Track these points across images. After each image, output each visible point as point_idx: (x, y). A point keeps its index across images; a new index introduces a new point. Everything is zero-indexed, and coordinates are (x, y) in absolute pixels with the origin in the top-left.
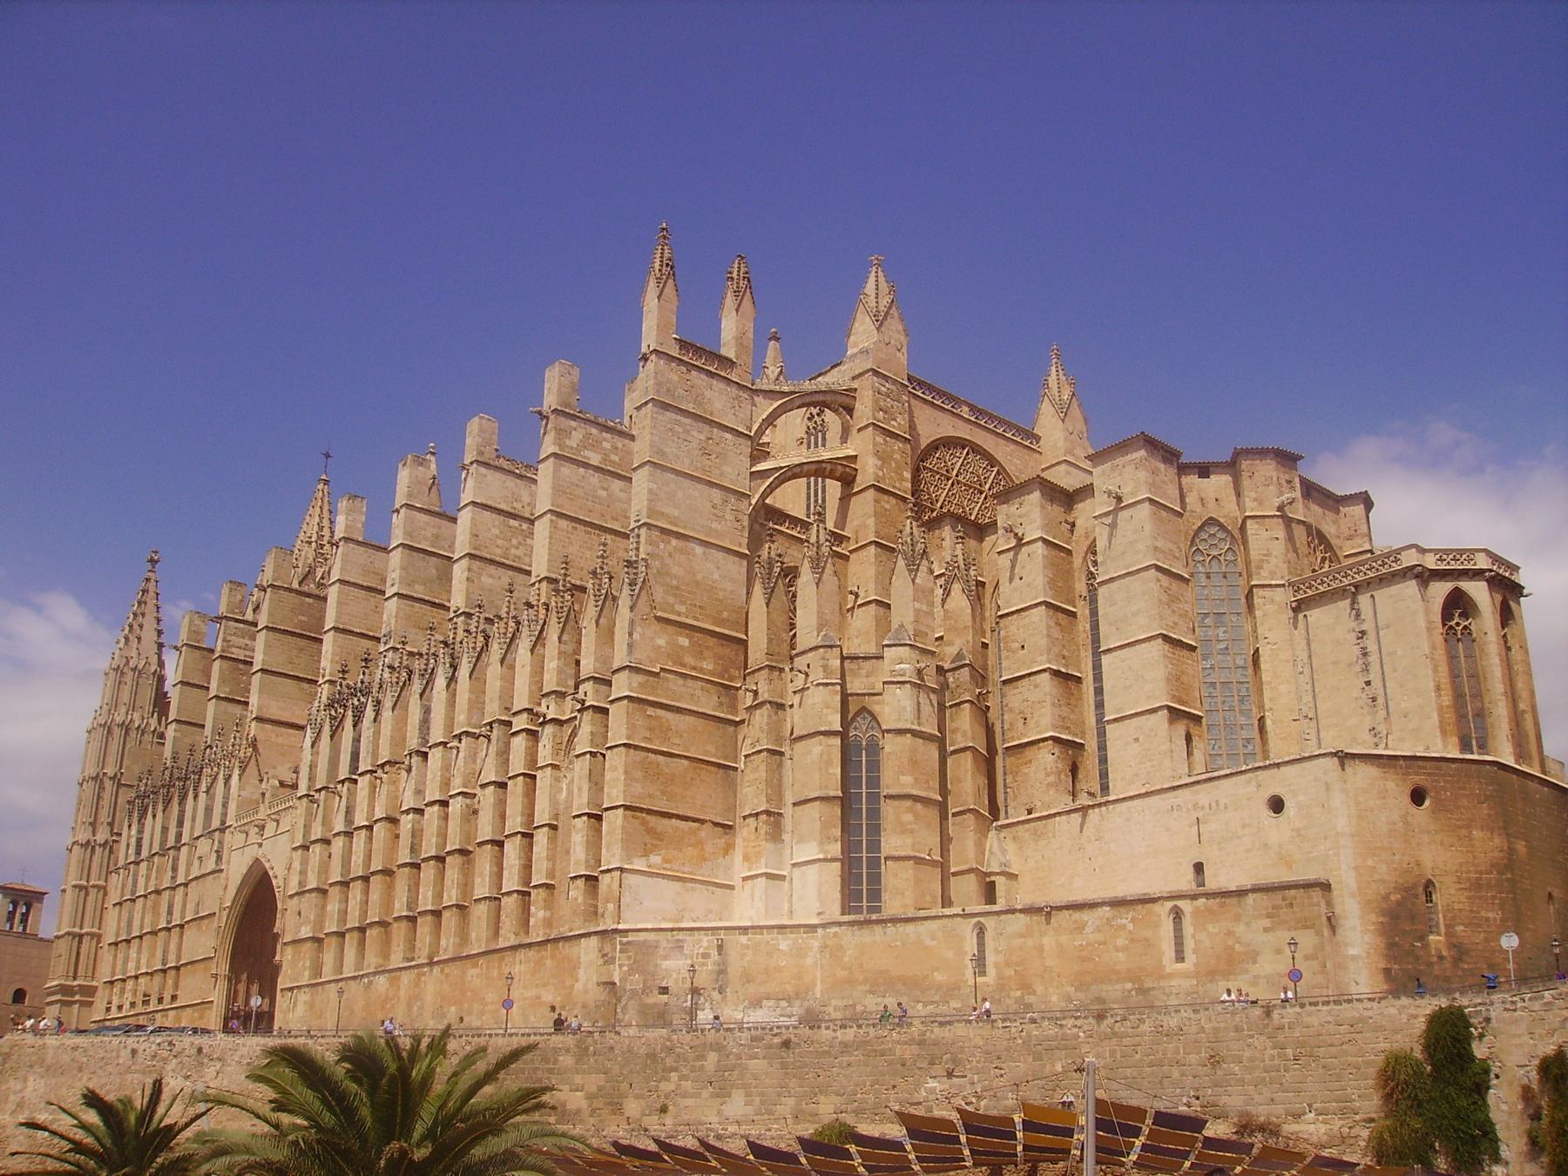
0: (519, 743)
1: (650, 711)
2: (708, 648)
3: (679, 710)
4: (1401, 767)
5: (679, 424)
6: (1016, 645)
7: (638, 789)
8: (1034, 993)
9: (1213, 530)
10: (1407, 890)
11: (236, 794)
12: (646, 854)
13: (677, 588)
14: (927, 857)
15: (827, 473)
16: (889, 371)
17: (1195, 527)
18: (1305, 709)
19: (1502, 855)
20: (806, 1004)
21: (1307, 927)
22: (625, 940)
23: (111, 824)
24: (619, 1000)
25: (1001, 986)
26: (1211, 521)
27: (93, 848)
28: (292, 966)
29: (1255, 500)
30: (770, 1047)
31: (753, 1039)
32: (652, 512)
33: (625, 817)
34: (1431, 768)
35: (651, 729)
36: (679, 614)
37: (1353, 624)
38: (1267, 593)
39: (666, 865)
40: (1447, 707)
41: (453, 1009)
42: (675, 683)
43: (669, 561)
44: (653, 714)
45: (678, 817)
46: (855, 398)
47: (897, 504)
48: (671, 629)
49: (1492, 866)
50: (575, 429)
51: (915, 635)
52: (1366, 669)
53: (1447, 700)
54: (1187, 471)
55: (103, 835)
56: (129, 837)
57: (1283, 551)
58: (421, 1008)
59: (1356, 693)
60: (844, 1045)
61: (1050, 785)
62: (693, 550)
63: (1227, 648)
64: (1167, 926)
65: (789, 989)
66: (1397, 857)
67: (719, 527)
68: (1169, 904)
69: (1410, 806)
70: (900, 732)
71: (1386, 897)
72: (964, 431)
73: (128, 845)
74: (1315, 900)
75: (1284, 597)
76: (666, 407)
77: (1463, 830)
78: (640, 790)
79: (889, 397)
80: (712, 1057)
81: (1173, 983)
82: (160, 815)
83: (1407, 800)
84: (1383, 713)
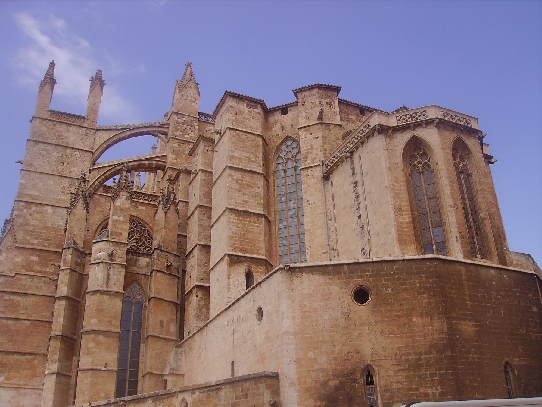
1: (6, 297)
3: (26, 294)
4: (345, 273)
5: (45, 150)
6: (191, 234)
9: (289, 143)
10: (345, 376)
13: (33, 231)
14: (103, 369)
15: (147, 166)
17: (278, 144)
18: (332, 244)
19: (441, 336)
26: (288, 138)
34: (373, 271)
35: (5, 307)
36: (33, 244)
37: (352, 179)
38: (309, 172)
40: (407, 223)
42: (25, 281)
43: (29, 218)
44: (7, 298)
46: (168, 128)
48: (26, 253)
49: (431, 346)
51: (111, 235)
52: (358, 208)
53: (406, 218)
54: (275, 113)
59: (355, 226)
62: (47, 211)
63: (295, 214)
66: (338, 348)
67: (66, 198)
68: (180, 397)
69: (352, 304)
70: (94, 292)
71: (325, 384)
74: (261, 391)
75: (318, 173)
76: (37, 142)
77: (402, 319)
79: (184, 124)
83: (349, 299)
84: (366, 238)
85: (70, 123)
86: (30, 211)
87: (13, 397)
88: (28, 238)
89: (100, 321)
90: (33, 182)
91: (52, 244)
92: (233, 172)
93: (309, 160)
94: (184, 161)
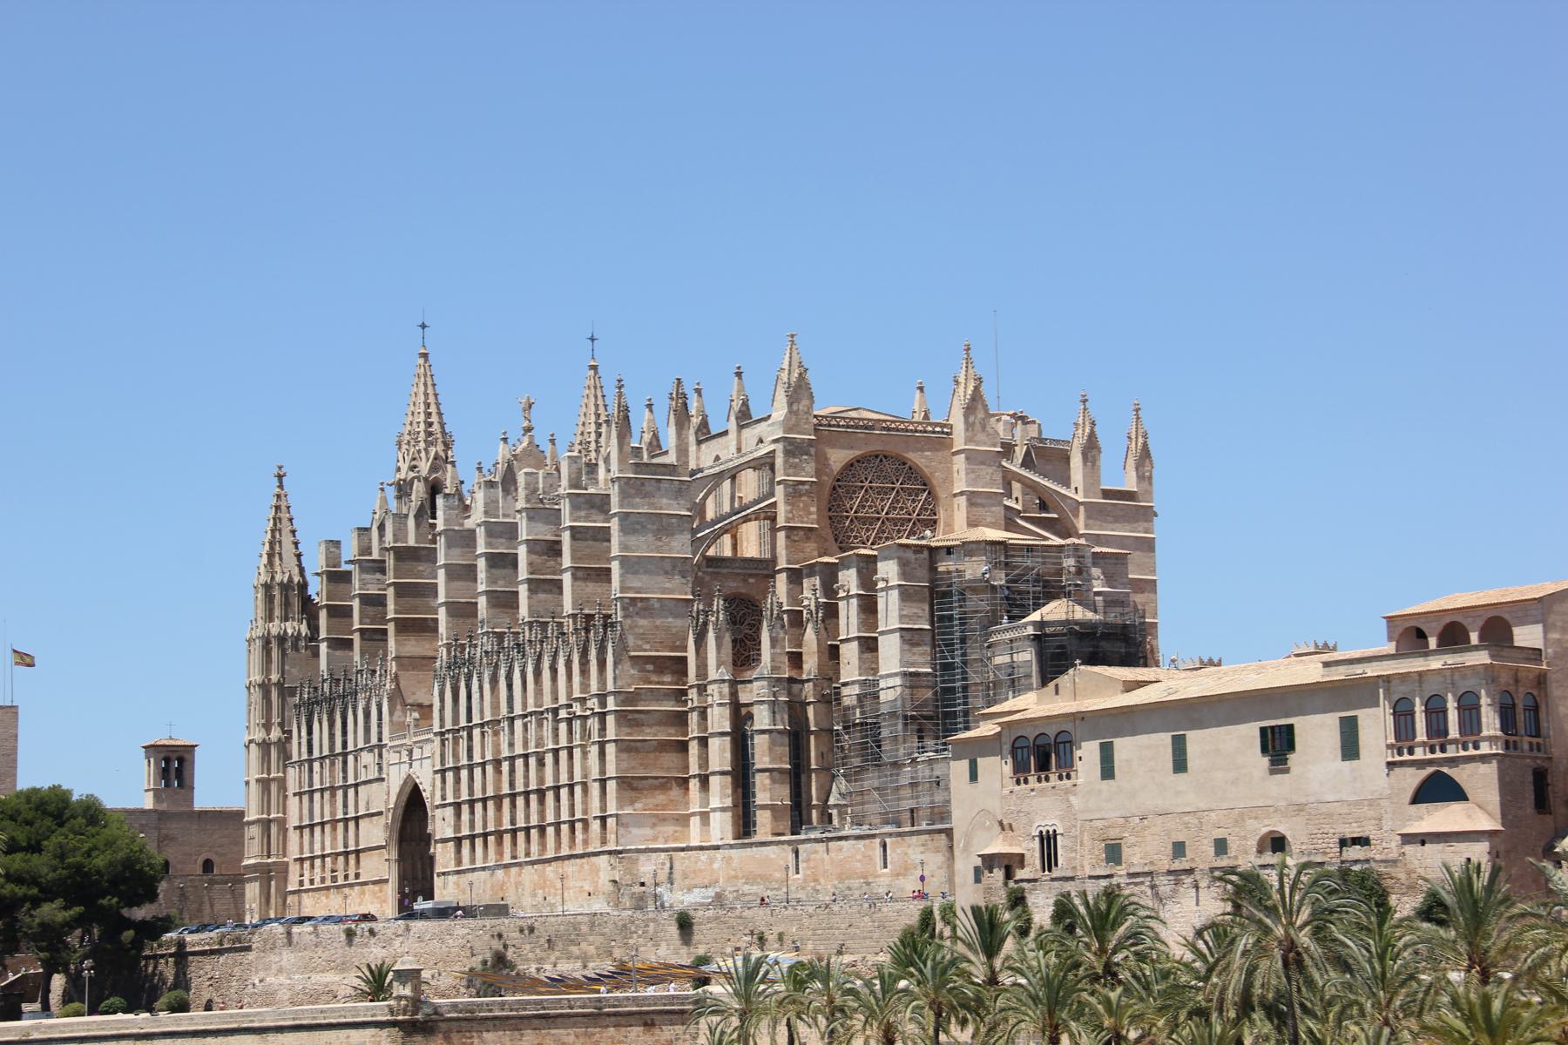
0: (563, 727)
2: (666, 668)
5: (638, 523)
6: (846, 661)
7: (624, 765)
12: (632, 803)
13: (643, 634)
21: (938, 852)
23: (281, 725)
24: (619, 890)
25: (805, 881)
28: (443, 856)
41: (540, 891)
45: (652, 777)
55: (275, 734)
58: (523, 890)
60: (708, 918)
64: (878, 851)
65: (706, 882)
70: (763, 732)
73: (300, 743)
80: (652, 925)
81: (882, 879)
86: (637, 610)
88: (640, 643)
91: (665, 647)
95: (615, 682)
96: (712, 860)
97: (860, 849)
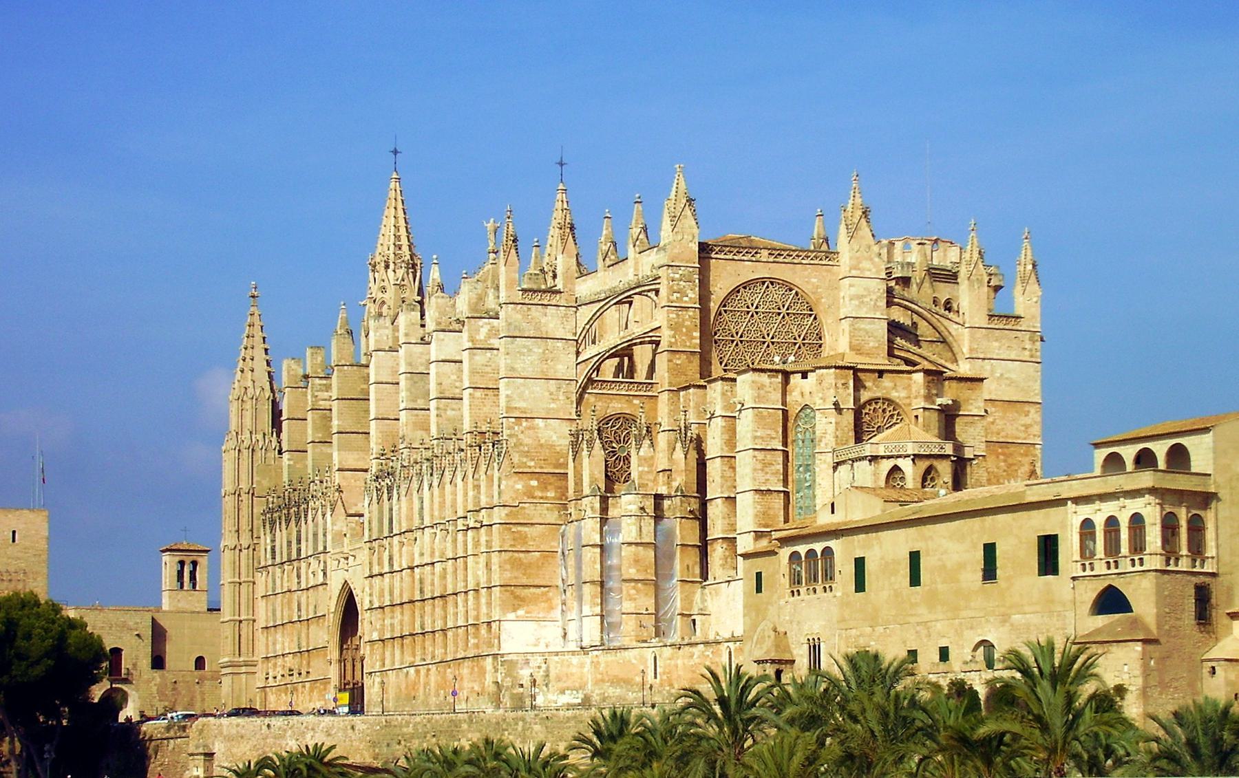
1: (514, 529)
2: (550, 484)
5: (525, 347)
7: (508, 575)
8: (674, 688)
9: (809, 411)
11: (331, 529)
12: (515, 610)
13: (528, 452)
16: (682, 261)
17: (797, 411)
20: (585, 692)
22: (503, 659)
25: (661, 685)
27: (240, 550)
29: (821, 399)
30: (542, 719)
31: (536, 715)
32: (509, 409)
33: (501, 592)
36: (530, 467)
39: (527, 615)
43: (521, 436)
47: (687, 358)
50: (482, 327)
56: (266, 544)
57: (834, 431)
58: (429, 690)
61: (721, 565)
62: (538, 425)
65: (577, 685)
68: (726, 644)
72: (762, 271)
75: (829, 459)
78: (509, 575)
80: (521, 723)
82: (284, 531)
85: (545, 302)
87: (536, 630)
88: (525, 460)
89: (638, 571)
90: (519, 391)
91: (548, 464)
92: (756, 453)
93: (822, 445)
94: (684, 338)
95: (499, 498)
96: (582, 665)
97: (708, 656)
